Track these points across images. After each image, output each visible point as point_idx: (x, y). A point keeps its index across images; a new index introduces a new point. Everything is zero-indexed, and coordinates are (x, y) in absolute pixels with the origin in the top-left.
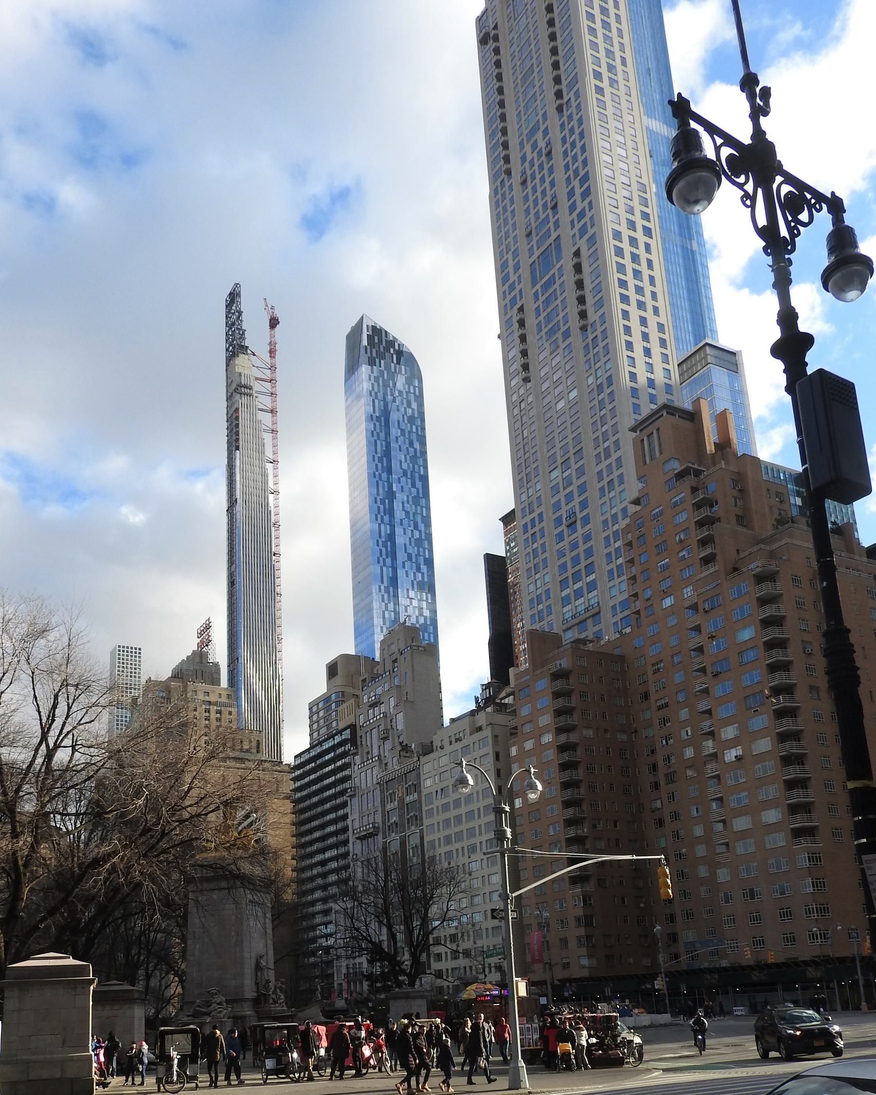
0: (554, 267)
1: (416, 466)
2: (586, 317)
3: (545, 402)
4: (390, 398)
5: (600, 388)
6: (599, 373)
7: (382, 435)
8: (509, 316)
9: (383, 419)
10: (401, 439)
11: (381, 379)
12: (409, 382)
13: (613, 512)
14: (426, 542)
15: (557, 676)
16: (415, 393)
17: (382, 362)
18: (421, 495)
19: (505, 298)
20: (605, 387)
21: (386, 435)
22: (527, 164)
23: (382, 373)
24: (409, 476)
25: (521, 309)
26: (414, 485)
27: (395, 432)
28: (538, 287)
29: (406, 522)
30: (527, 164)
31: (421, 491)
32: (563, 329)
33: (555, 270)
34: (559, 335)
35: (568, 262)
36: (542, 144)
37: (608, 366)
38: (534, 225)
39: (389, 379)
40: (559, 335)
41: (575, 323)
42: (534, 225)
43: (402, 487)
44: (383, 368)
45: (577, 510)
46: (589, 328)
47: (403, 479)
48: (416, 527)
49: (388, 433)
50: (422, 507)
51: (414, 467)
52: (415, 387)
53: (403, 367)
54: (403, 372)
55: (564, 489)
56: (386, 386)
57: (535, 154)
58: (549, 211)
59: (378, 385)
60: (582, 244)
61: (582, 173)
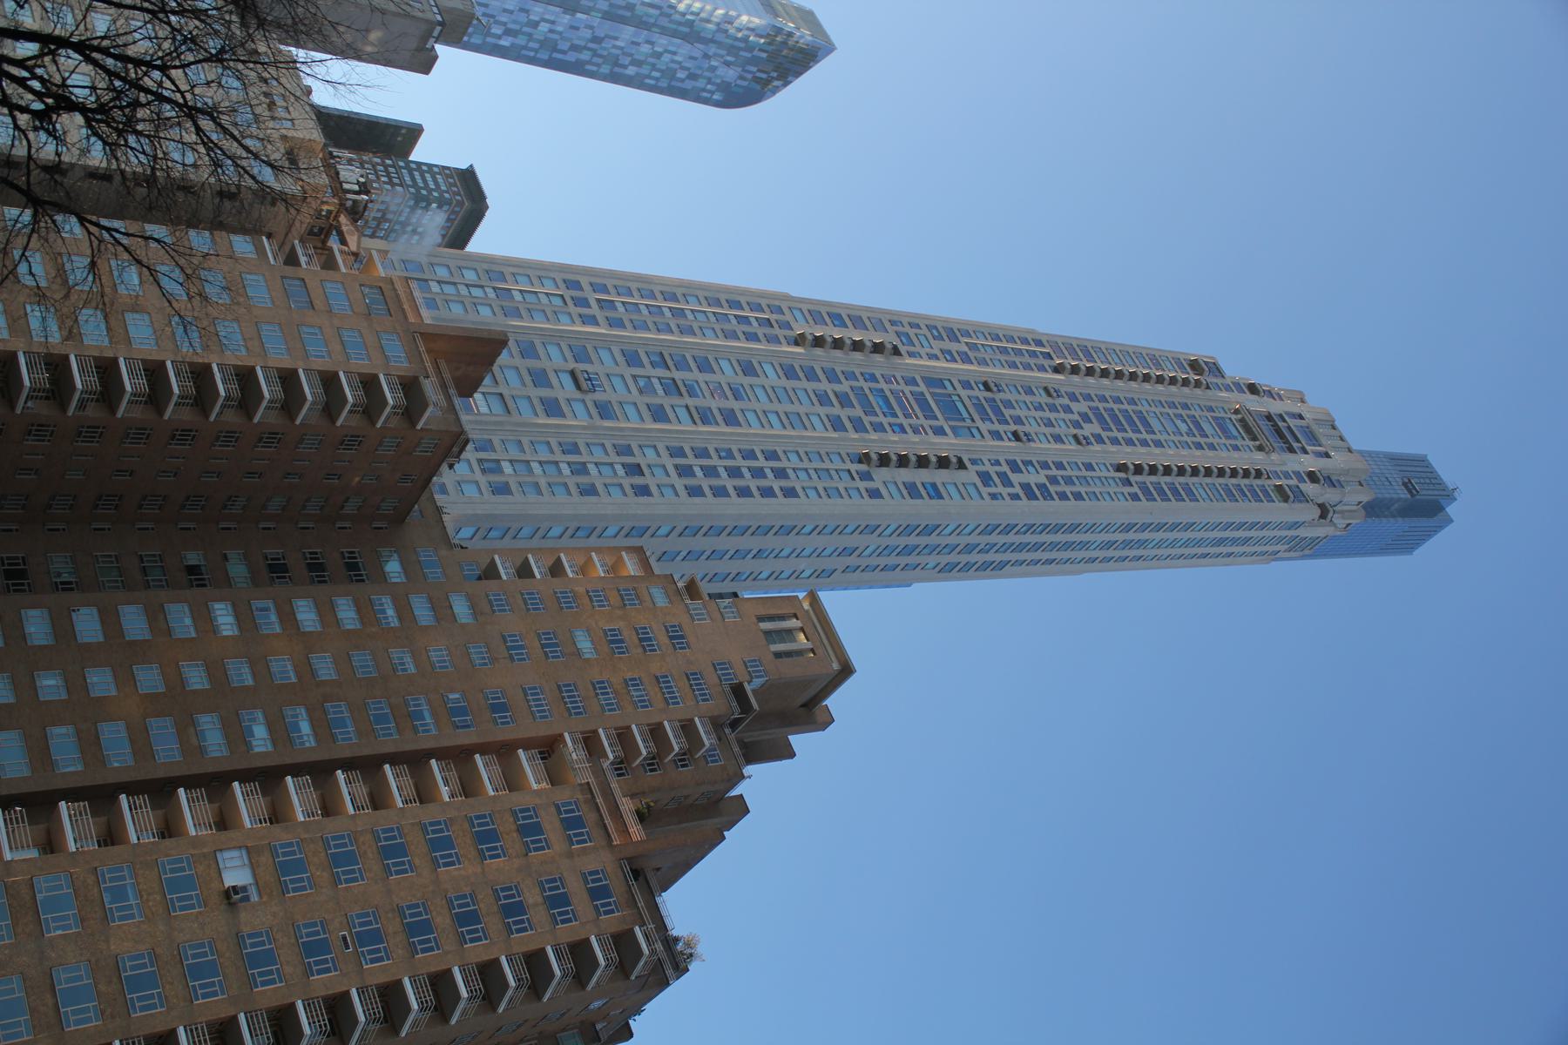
0: (947, 419)
1: (600, 61)
2: (881, 465)
3: (768, 368)
4: (712, 50)
5: (781, 474)
6: (802, 475)
7: (664, 22)
8: (888, 325)
9: (628, 14)
10: (646, 48)
11: (742, 45)
12: (725, 87)
13: (591, 467)
14: (479, 41)
15: (410, 387)
16: (704, 90)
17: (764, 55)
18: (555, 55)
19: (911, 325)
20: (784, 483)
21: (663, 28)
22: (1066, 401)
23: (750, 48)
24: (590, 45)
25: (896, 351)
26: (574, 48)
27: (662, 42)
28: (922, 388)
29: (523, 18)
30: (1066, 401)
31: (560, 56)
32: (866, 420)
33: (941, 422)
34: (858, 412)
35: (947, 444)
36: (1089, 429)
37: (812, 493)
38: (998, 396)
39: (736, 56)
40: (858, 412)
41: (875, 443)
42: (998, 396)
43: (577, 29)
44: (756, 53)
45: (598, 396)
46: (863, 467)
47: (588, 34)
48: (508, 32)
49: (664, 31)
50: (536, 51)
51: (600, 56)
52: (712, 93)
53: (745, 83)
54: (739, 82)
55: (634, 377)
56: (732, 50)
57: (1076, 417)
58: (1013, 427)
59: (680, 24)
60: (970, 475)
61: (1052, 489)
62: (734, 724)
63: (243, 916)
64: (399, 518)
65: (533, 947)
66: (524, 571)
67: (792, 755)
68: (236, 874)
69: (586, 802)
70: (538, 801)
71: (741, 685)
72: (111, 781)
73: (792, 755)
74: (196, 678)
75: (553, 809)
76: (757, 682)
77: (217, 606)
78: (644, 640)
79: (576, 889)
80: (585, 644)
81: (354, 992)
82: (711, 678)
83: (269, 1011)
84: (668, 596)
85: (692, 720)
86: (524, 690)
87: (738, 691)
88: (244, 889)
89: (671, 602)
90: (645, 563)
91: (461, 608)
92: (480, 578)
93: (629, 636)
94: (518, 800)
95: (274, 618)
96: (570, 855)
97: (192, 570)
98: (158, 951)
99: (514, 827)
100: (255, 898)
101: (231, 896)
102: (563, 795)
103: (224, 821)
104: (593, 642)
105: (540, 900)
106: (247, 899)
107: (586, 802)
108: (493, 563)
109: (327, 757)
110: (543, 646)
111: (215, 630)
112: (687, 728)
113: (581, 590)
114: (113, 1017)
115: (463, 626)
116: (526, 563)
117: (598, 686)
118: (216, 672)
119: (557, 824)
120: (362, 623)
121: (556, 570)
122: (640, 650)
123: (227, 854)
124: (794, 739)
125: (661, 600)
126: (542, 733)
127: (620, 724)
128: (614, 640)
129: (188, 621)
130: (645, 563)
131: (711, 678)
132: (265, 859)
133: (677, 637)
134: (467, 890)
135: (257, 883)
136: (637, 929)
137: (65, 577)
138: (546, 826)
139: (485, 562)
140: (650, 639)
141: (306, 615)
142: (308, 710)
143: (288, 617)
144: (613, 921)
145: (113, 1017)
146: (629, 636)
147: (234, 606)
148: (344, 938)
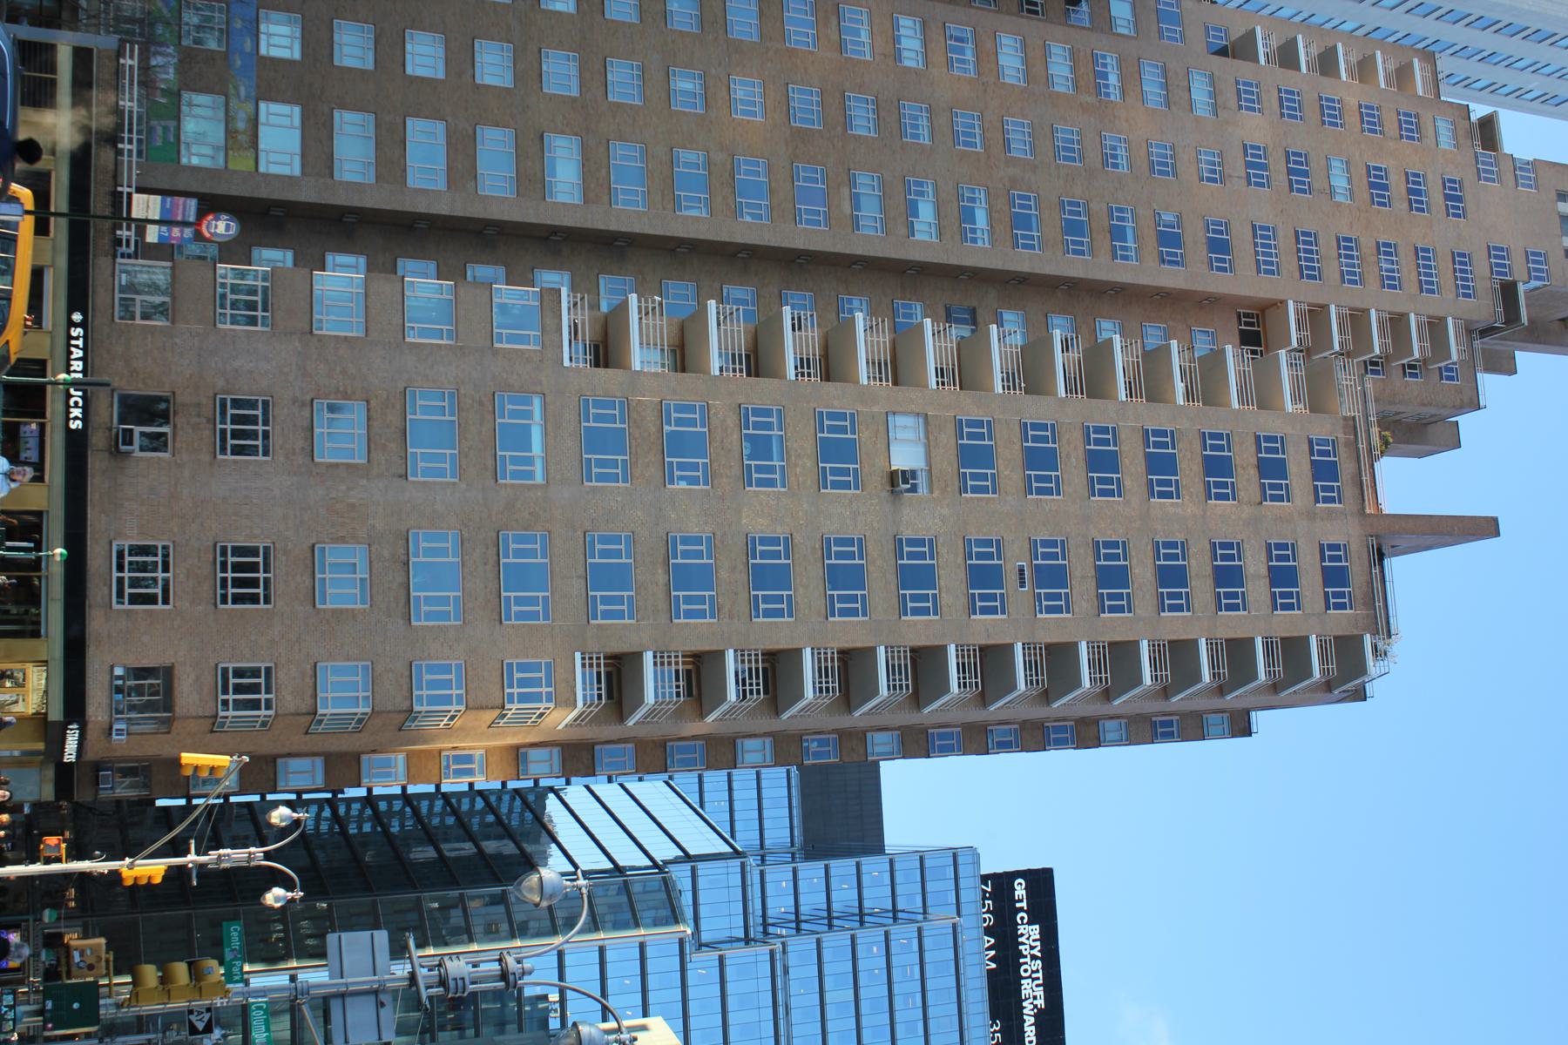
62: (1486, 332)
63: (907, 513)
65: (1240, 634)
66: (1286, 56)
67: (1512, 371)
68: (906, 455)
69: (1347, 444)
70: (1289, 430)
71: (1514, 285)
72: (739, 240)
73: (1512, 371)
74: (863, 122)
75: (1306, 447)
76: (1534, 283)
77: (905, 22)
78: (1415, 192)
79: (1309, 567)
80: (1340, 182)
81: (1019, 648)
82: (1481, 266)
83: (913, 650)
84: (1455, 137)
85: (1443, 320)
86: (1254, 227)
87: (1508, 292)
88: (913, 473)
89: (1457, 146)
90: (1435, 81)
91: (1200, 92)
93: (1397, 186)
94: (1269, 424)
95: (969, 56)
96: (1311, 516)
98: (798, 539)
99: (1254, 461)
100: (923, 489)
101: (898, 481)
102: (1323, 428)
103: (898, 367)
104: (1350, 181)
105: (1264, 571)
106: (914, 489)
107: (1347, 444)
108: (1251, 34)
109: (1000, 267)
110: (1290, 172)
111: (897, 56)
112: (1435, 327)
113: (1351, 101)
114: (731, 617)
115: (1197, 119)
116: (1293, 43)
117: (1346, 245)
118: (888, 113)
119: (1306, 467)
120: (1076, 87)
121: (1326, 63)
122: (1406, 205)
123: (900, 420)
124: (1520, 356)
125: (1446, 141)
126: (1262, 295)
127: (1358, 305)
128: (1377, 184)
129: (864, 37)
130: (1435, 81)
131: (1481, 266)
132: (947, 438)
133: (1454, 198)
134: (1179, 538)
135: (930, 471)
136: (1368, 639)
138: (1292, 468)
139: (1237, 32)
140: (1419, 193)
141: (1010, 60)
142: (988, 194)
143: (987, 58)
144: (1340, 621)
145: (731, 617)
146: (1397, 186)
147: (924, 24)
148: (1021, 571)
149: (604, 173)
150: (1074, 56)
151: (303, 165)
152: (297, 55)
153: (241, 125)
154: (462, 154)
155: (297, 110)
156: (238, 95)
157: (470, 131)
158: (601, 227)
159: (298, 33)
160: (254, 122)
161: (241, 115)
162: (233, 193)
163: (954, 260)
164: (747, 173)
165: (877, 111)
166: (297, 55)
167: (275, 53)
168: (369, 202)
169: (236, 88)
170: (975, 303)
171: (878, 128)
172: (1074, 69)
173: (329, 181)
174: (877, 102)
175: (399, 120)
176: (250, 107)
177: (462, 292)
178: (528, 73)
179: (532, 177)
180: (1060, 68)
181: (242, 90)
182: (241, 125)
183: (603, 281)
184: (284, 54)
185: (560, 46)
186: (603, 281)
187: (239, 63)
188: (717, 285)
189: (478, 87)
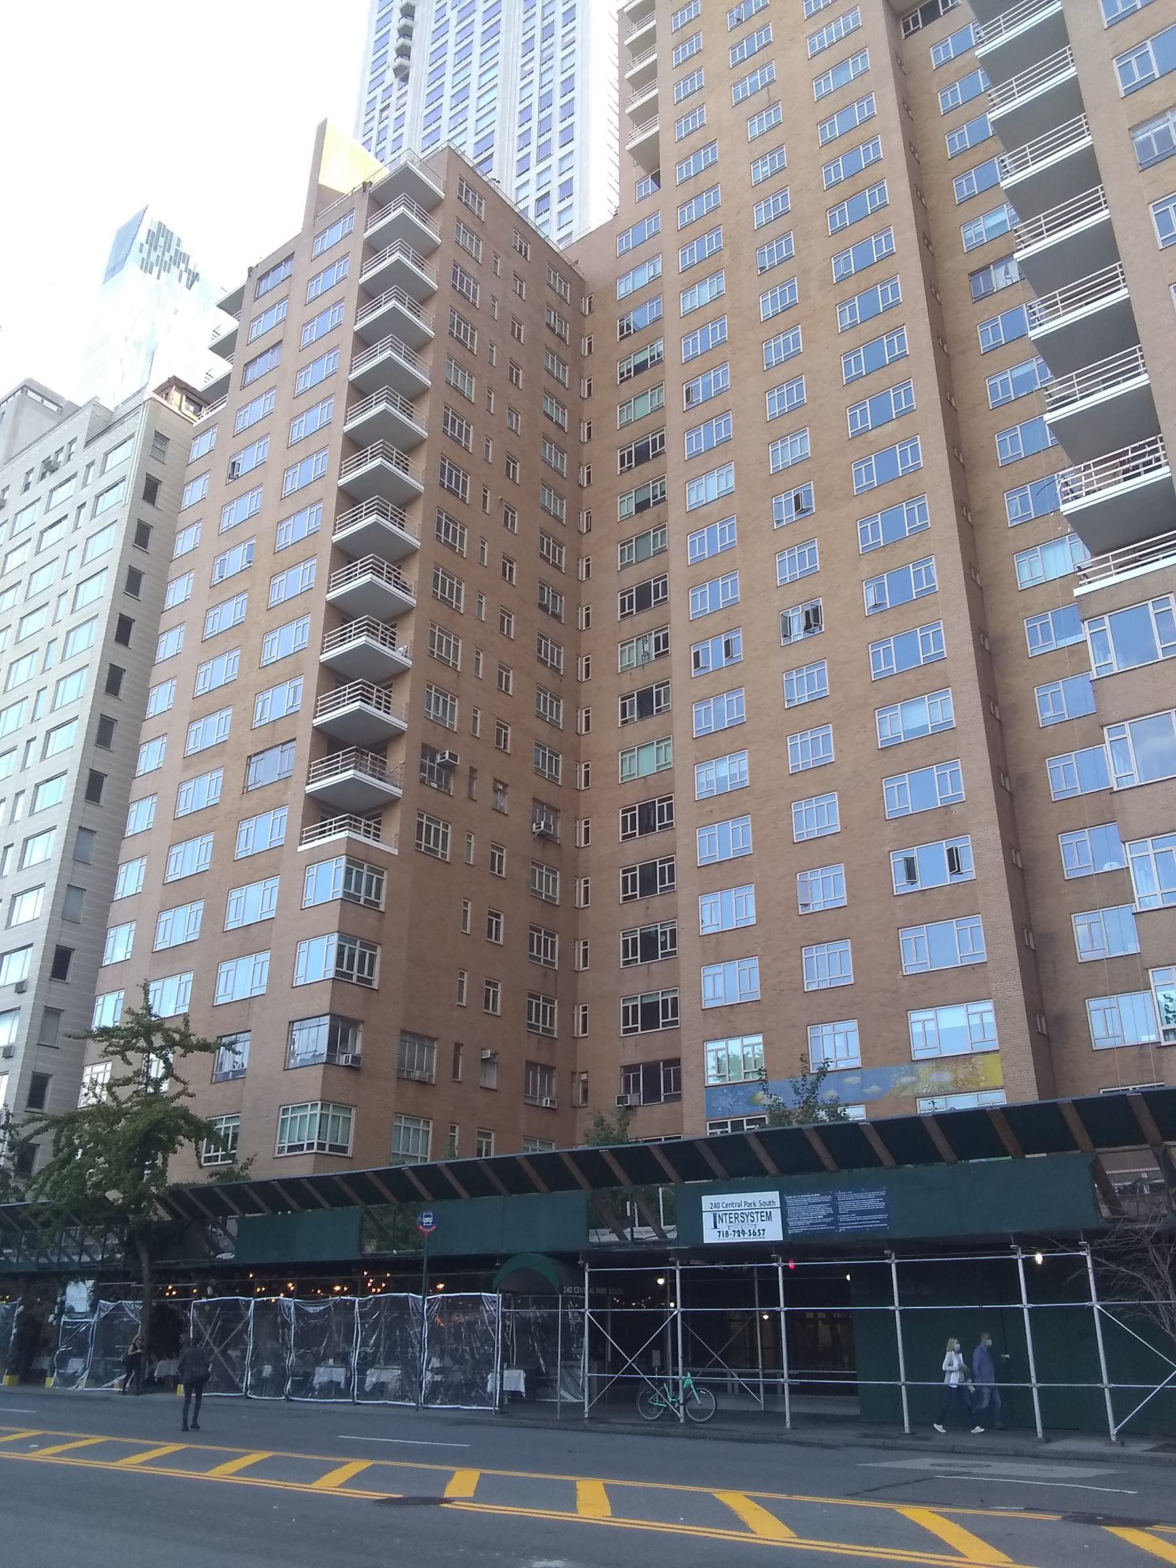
64: (578, 283)
92: (656, 178)
97: (641, 507)
137: (650, 646)
139: (640, 172)
149: (910, 676)
150: (689, 288)
151: (979, 999)
152: (853, 1025)
153: (947, 1077)
154: (933, 908)
155: (915, 1016)
156: (913, 1083)
157: (895, 824)
158: (972, 661)
159: (827, 1028)
160: (940, 1061)
161: (934, 1077)
162: (1032, 1075)
163: (923, 303)
164: (888, 661)
165: (783, 438)
166: (853, 1025)
167: (855, 1050)
168: (1006, 918)
169: (904, 1088)
170: (964, 277)
171: (801, 430)
172: (701, 281)
173: (990, 966)
174: (773, 442)
175: (900, 902)
176: (923, 1069)
177: (1114, 715)
178: (819, 779)
179: (934, 746)
180: (704, 294)
181: (906, 1080)
182: (947, 1077)
183: (1034, 651)
184: (854, 1038)
185: (783, 757)
186: (1034, 651)
187: (875, 1088)
188: (1010, 533)
189: (844, 827)
